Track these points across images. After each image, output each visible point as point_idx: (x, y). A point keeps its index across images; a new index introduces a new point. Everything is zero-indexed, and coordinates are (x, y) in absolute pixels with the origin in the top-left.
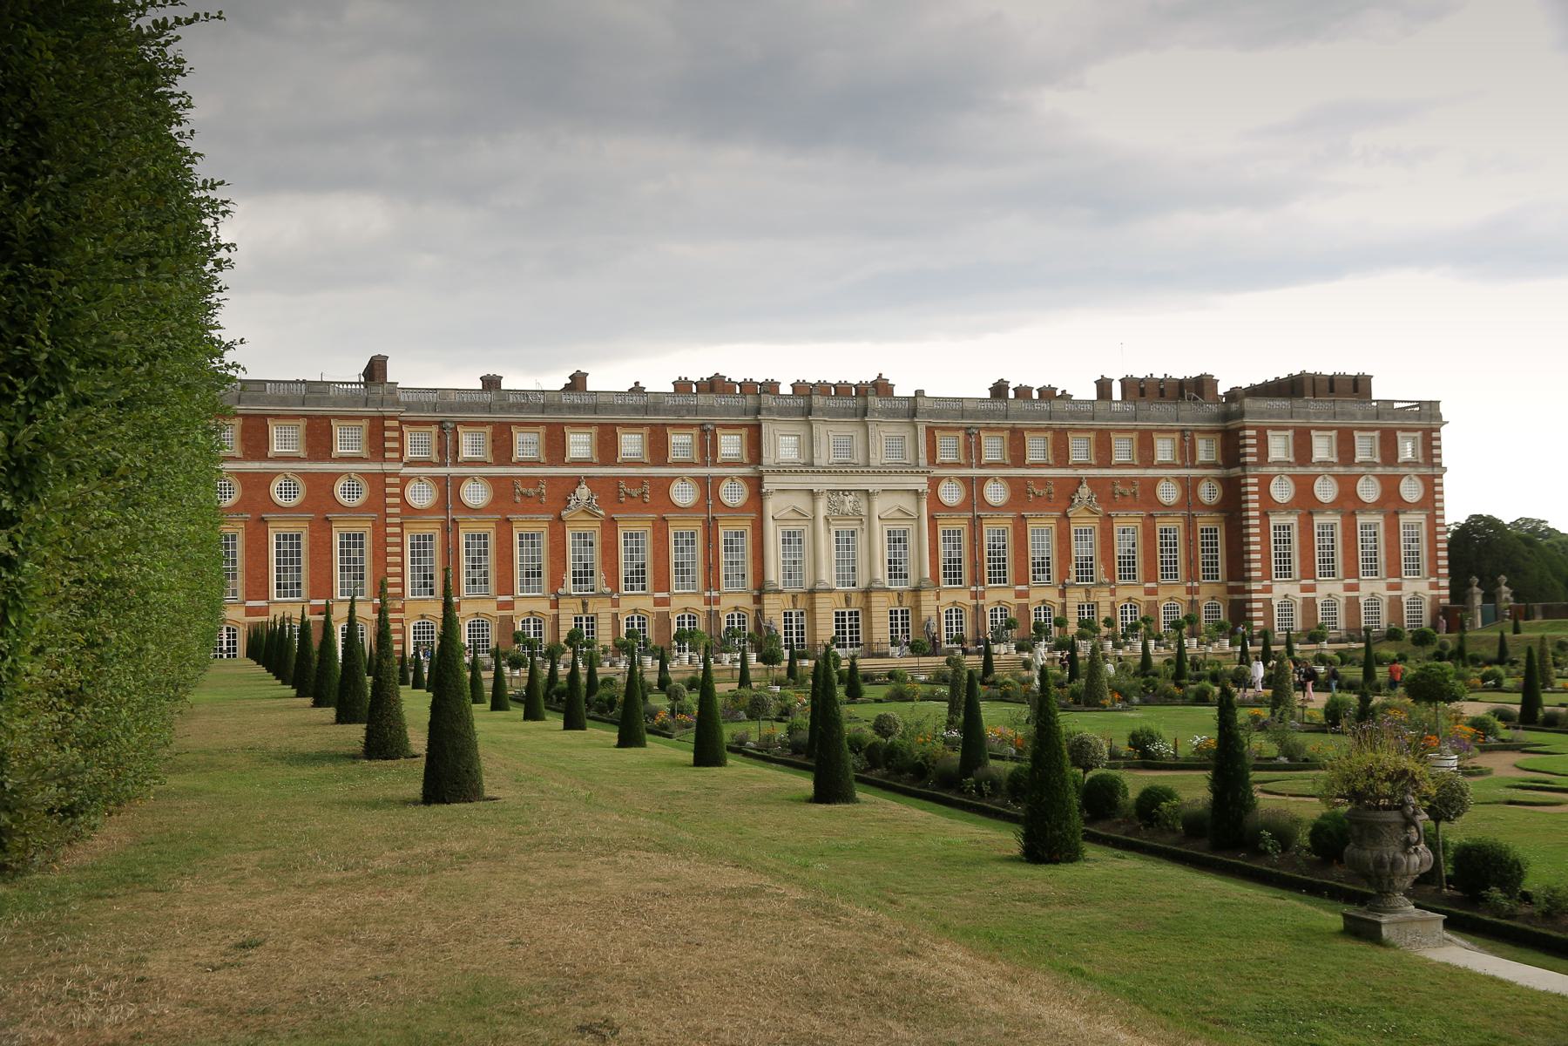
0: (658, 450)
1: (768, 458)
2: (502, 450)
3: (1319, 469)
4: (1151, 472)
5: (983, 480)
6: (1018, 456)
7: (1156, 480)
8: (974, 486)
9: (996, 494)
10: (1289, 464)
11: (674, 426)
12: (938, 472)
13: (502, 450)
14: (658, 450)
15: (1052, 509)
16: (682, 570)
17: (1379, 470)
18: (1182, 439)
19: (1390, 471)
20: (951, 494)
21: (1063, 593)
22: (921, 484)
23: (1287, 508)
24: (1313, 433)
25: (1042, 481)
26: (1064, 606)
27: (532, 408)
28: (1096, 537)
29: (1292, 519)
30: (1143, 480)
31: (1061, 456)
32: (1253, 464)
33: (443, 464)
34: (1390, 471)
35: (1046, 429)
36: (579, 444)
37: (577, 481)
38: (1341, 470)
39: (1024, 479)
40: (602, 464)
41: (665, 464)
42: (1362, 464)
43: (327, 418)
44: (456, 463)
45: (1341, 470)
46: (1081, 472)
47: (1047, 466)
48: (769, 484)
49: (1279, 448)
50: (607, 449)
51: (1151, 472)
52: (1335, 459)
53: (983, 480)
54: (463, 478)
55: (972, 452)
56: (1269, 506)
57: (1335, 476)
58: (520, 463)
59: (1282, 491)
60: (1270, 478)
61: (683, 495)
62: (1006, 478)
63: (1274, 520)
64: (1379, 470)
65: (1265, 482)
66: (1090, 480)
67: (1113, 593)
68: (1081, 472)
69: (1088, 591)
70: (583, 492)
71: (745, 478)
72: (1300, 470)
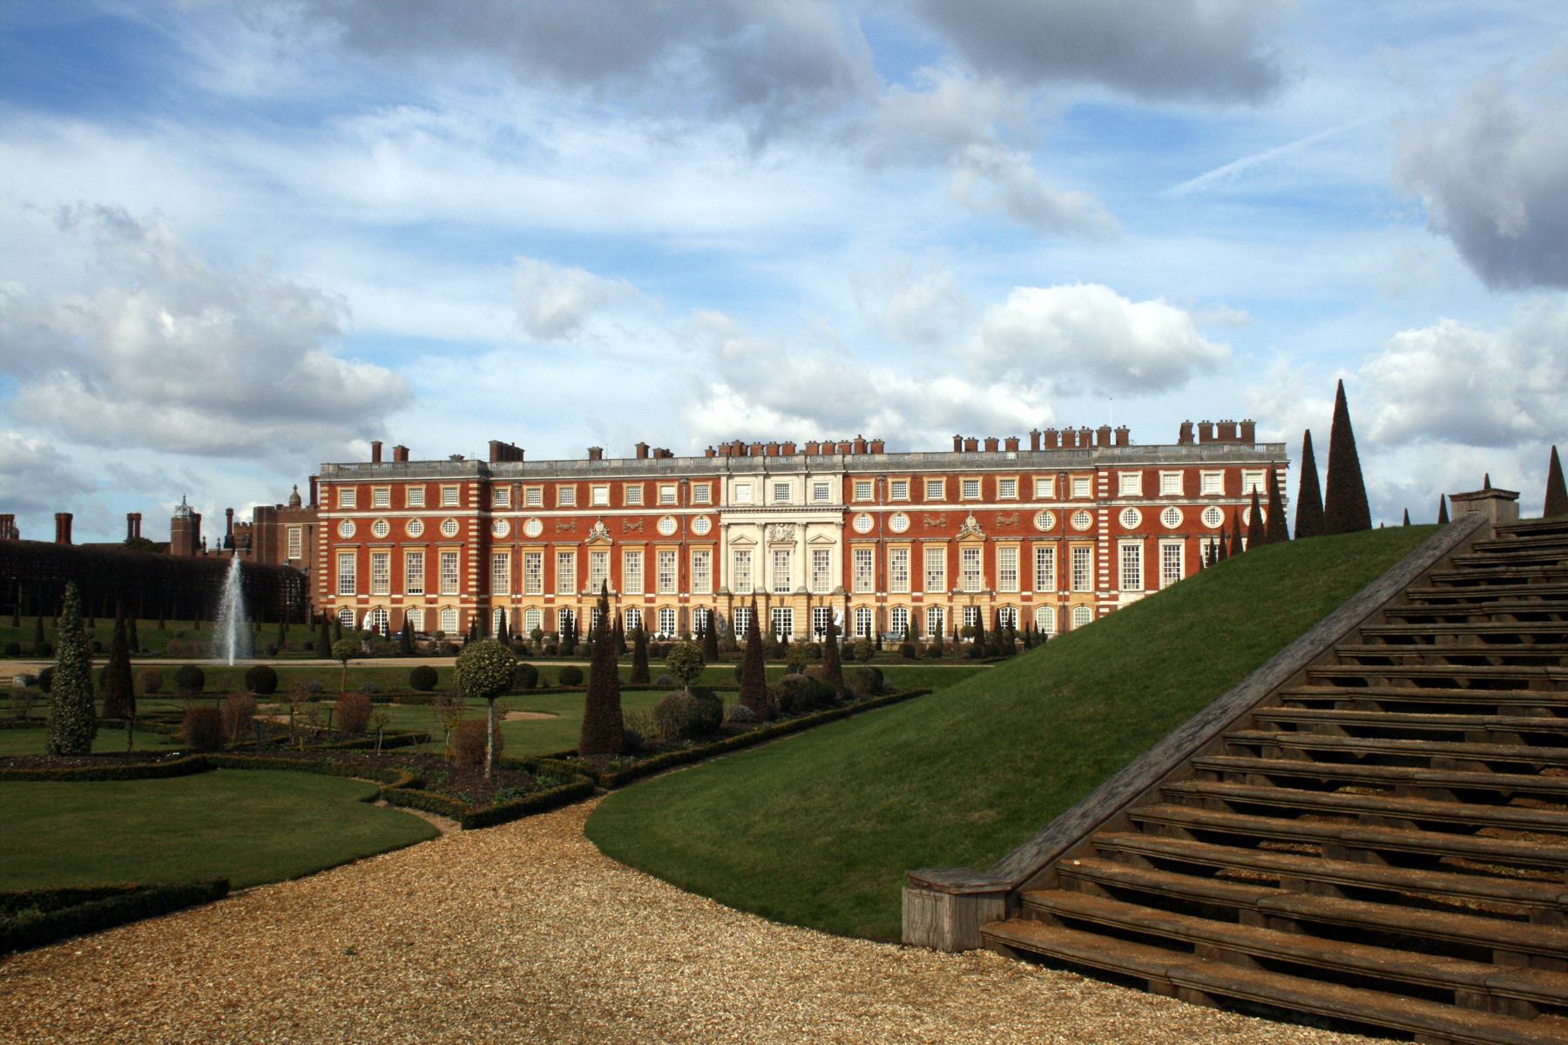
0: (650, 501)
1: (723, 503)
2: (550, 503)
3: (1165, 502)
4: (1028, 506)
5: (888, 514)
6: (917, 497)
7: (1034, 512)
8: (882, 519)
9: (899, 524)
10: (1136, 498)
11: (662, 480)
12: (853, 508)
13: (550, 503)
14: (650, 501)
15: (945, 535)
16: (666, 579)
17: (1222, 501)
18: (1058, 481)
19: (1232, 502)
20: (864, 525)
21: (950, 599)
22: (838, 517)
23: (1135, 534)
24: (1162, 473)
25: (935, 514)
26: (951, 609)
27: (563, 471)
28: (980, 557)
29: (1140, 543)
30: (1021, 513)
31: (953, 496)
32: (1105, 499)
33: (512, 510)
34: (1232, 502)
35: (943, 474)
36: (601, 495)
37: (594, 519)
38: (1185, 502)
39: (922, 512)
40: (613, 507)
41: (654, 507)
42: (1207, 497)
43: (437, 483)
44: (521, 509)
45: (1185, 502)
46: (968, 507)
47: (942, 502)
48: (726, 519)
49: (1131, 485)
50: (616, 499)
51: (1028, 506)
52: (1182, 493)
53: (888, 514)
54: (525, 519)
55: (881, 494)
56: (1116, 531)
57: (1182, 507)
58: (562, 508)
59: (1131, 519)
60: (1120, 509)
61: (667, 527)
62: (908, 513)
63: (1121, 543)
64: (1222, 501)
65: (1114, 513)
66: (975, 513)
67: (993, 598)
68: (968, 507)
69: (972, 599)
70: (599, 527)
71: (709, 515)
72: (1145, 502)
